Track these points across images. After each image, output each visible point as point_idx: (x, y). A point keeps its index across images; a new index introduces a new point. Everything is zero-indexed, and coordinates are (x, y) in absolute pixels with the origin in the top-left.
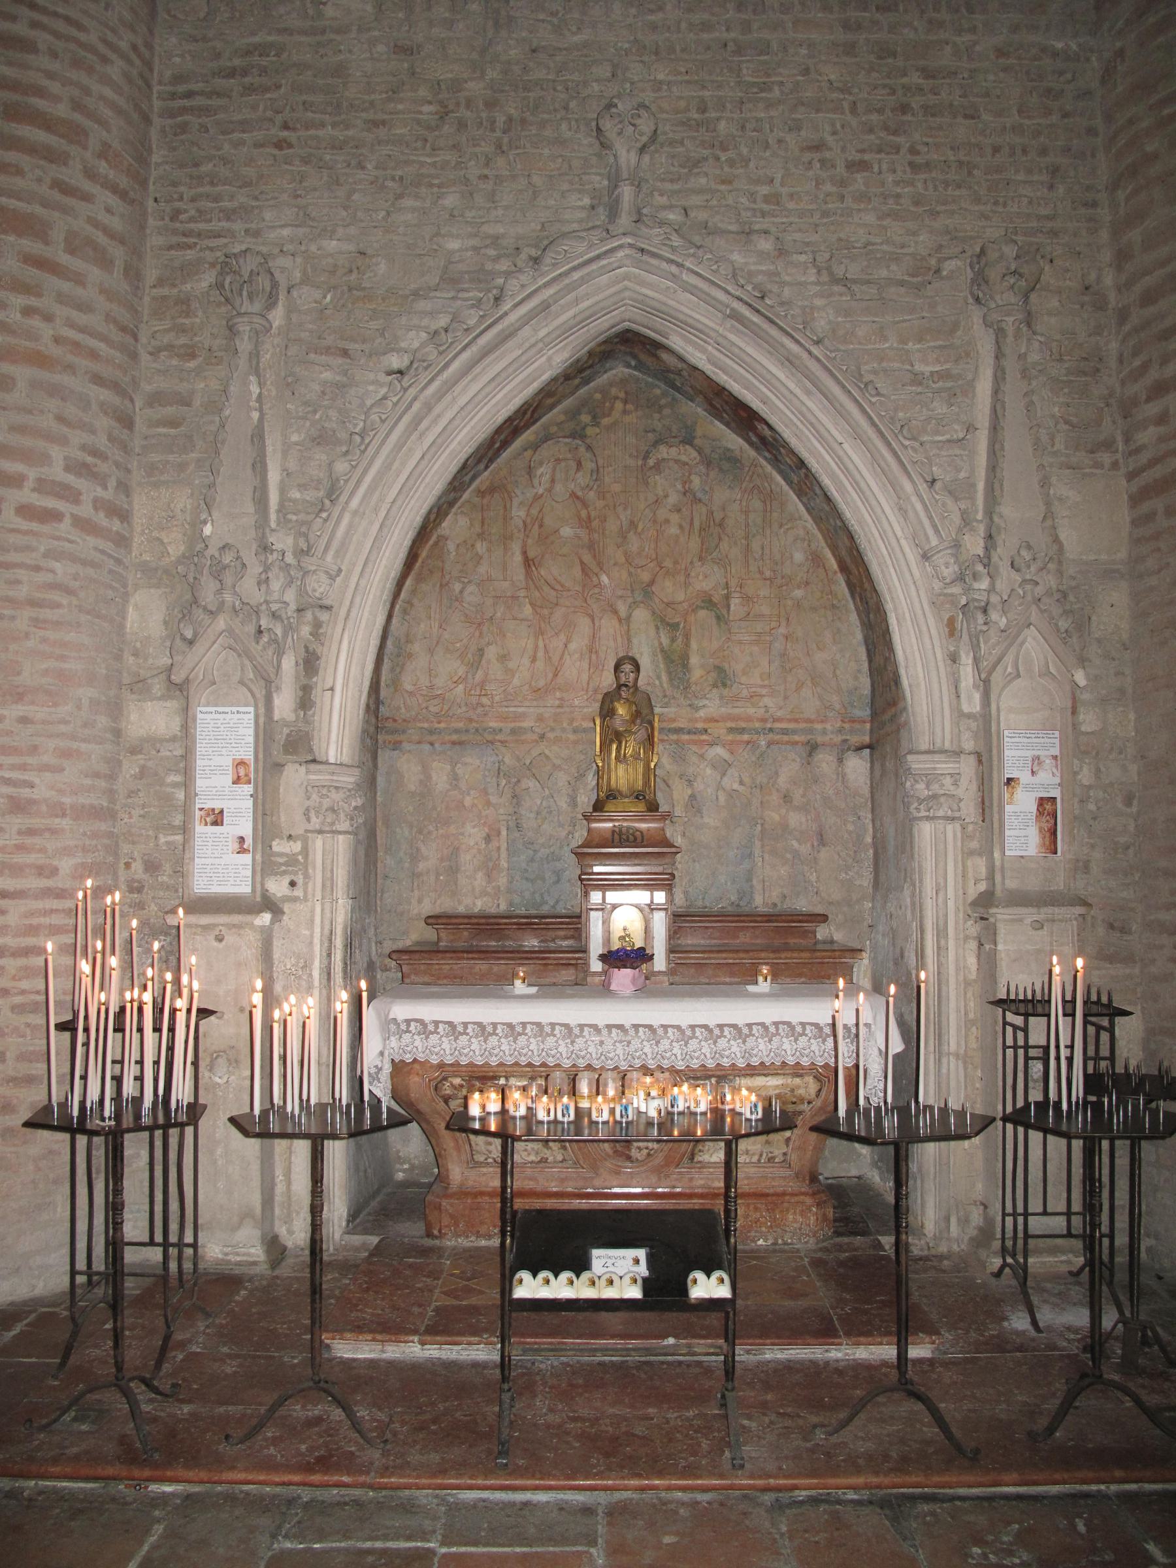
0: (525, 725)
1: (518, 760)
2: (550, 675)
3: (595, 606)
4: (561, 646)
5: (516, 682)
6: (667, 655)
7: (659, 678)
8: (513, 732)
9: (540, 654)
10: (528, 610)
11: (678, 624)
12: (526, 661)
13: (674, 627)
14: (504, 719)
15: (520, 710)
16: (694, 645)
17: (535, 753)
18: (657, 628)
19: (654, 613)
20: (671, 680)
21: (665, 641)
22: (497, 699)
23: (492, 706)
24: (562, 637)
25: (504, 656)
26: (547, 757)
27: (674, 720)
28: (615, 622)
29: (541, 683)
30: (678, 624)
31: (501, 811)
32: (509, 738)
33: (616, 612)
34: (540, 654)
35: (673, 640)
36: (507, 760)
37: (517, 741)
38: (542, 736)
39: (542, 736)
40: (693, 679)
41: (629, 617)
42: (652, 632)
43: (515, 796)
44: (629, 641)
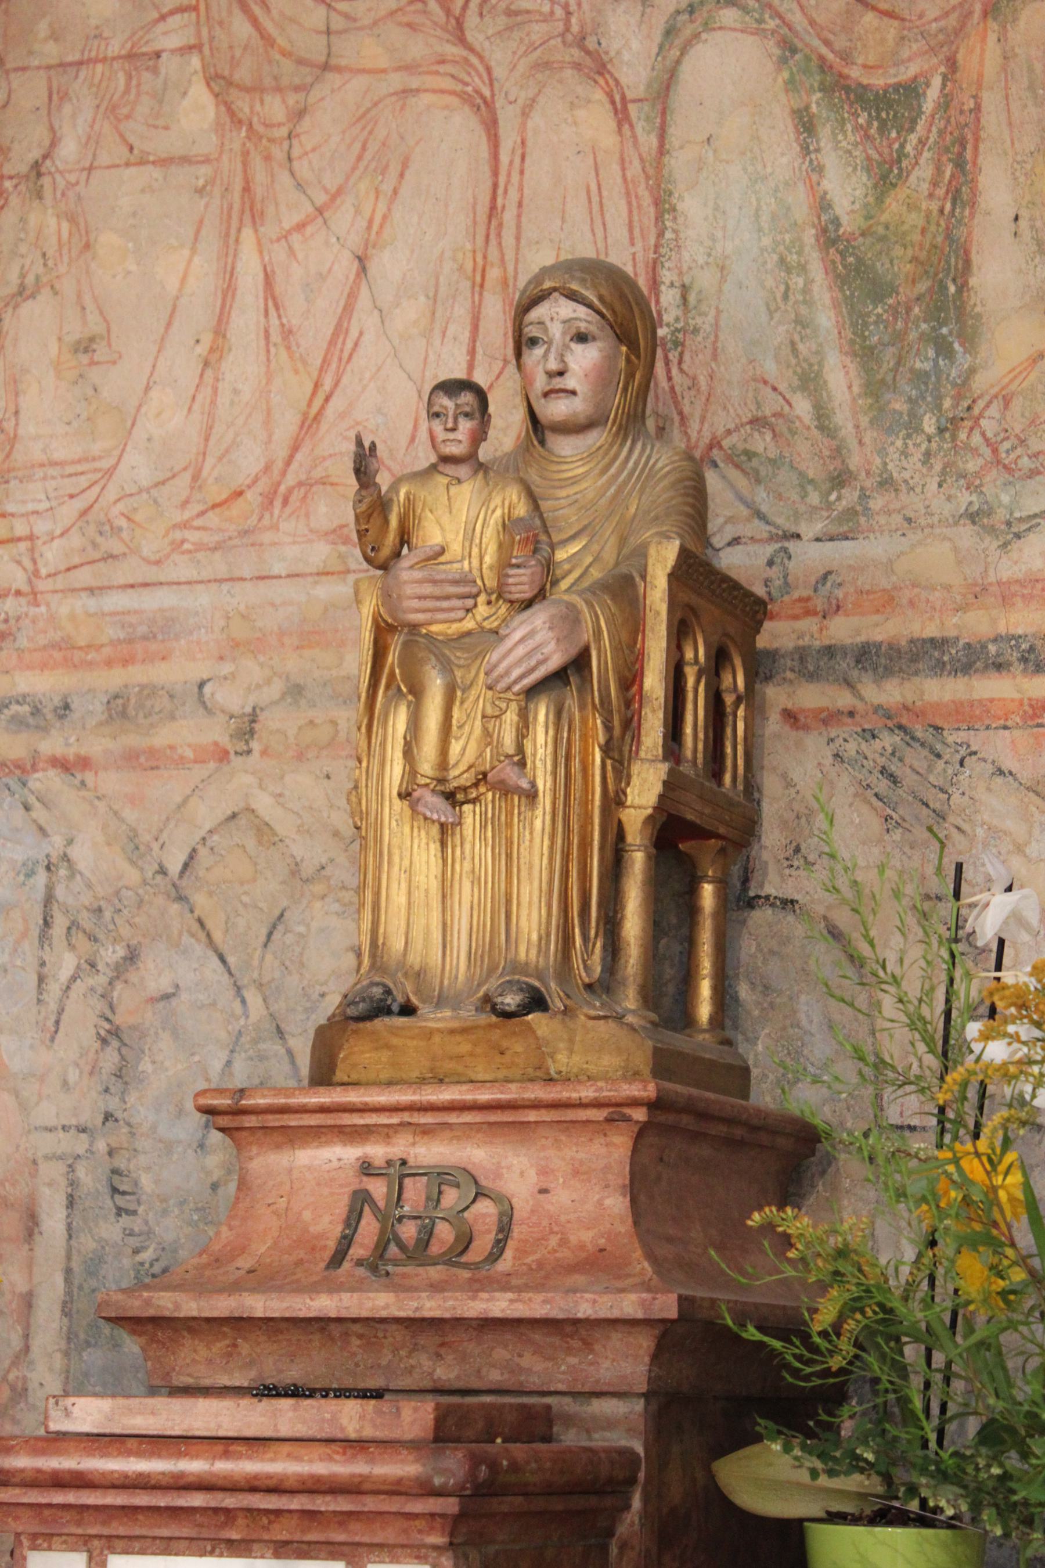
0: (160, 674)
1: (134, 848)
2: (287, 424)
3: (499, 56)
4: (345, 266)
5: (138, 467)
6: (855, 268)
7: (810, 381)
8: (120, 709)
9: (246, 320)
10: (196, 112)
11: (911, 91)
12: (182, 364)
13: (890, 107)
14: (66, 653)
15: (151, 601)
16: (996, 190)
17: (207, 813)
18: (806, 124)
19: (789, 47)
20: (875, 389)
21: (846, 190)
22: (51, 556)
23: (34, 597)
24: (345, 220)
25: (85, 346)
26: (264, 831)
27: (887, 602)
28: (596, 122)
29: (249, 461)
30: (911, 91)
31: (47, 1113)
32: (96, 746)
33: (598, 67)
34: (246, 320)
35: (886, 176)
36: (81, 854)
37: (131, 758)
38: (247, 727)
39: (247, 727)
40: (980, 382)
41: (664, 88)
42: (781, 154)
43: (112, 1034)
44: (663, 205)
